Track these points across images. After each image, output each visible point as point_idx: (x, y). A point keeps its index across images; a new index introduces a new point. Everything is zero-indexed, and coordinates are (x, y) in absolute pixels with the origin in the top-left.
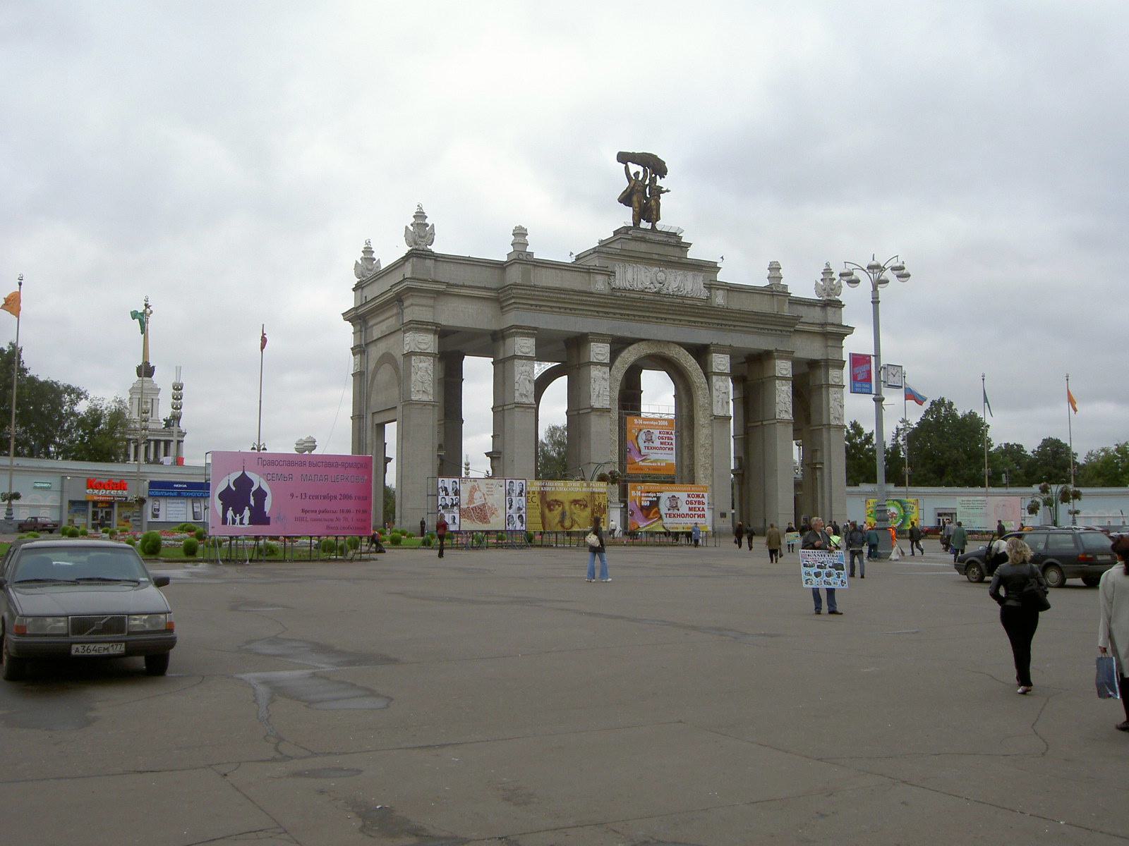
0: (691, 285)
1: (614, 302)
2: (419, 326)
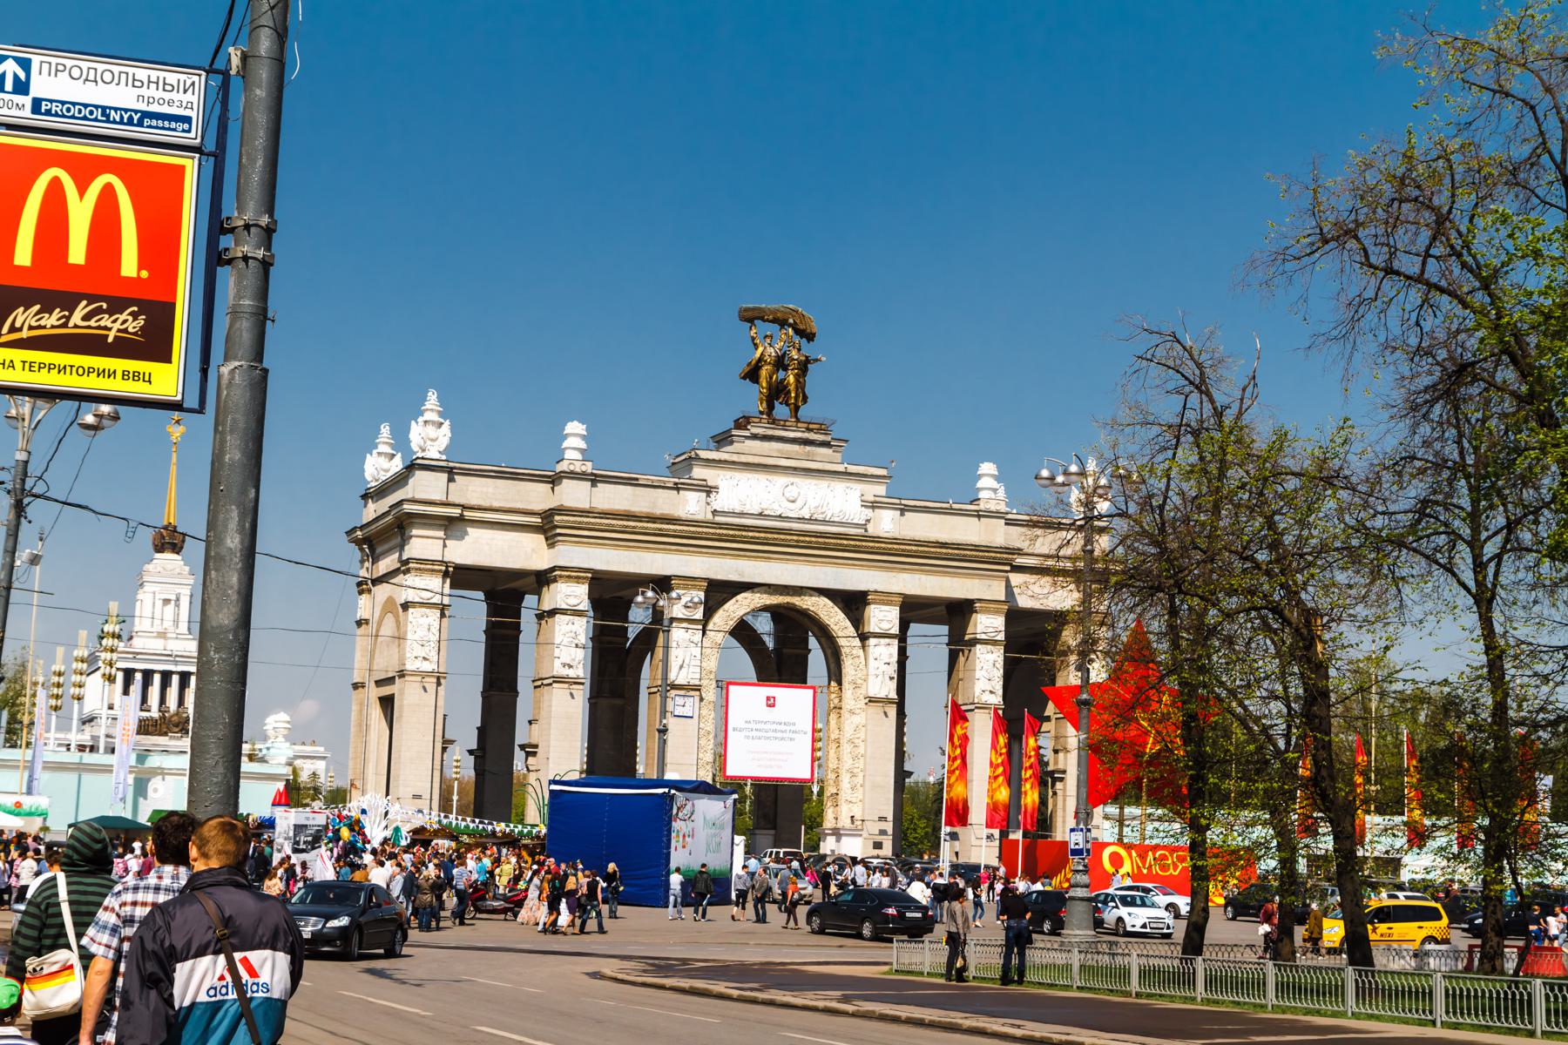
0: (839, 502)
2: (426, 566)
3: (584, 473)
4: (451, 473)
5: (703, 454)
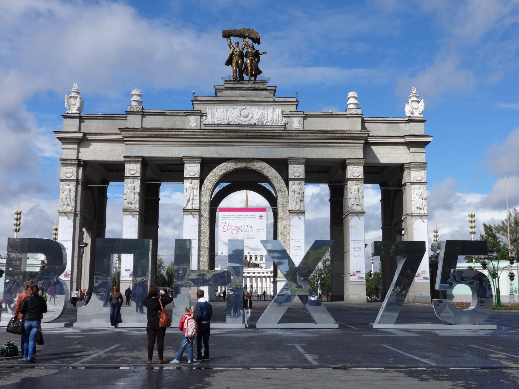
0: (271, 116)
1: (201, 133)
3: (138, 112)
4: (81, 119)
5: (199, 98)
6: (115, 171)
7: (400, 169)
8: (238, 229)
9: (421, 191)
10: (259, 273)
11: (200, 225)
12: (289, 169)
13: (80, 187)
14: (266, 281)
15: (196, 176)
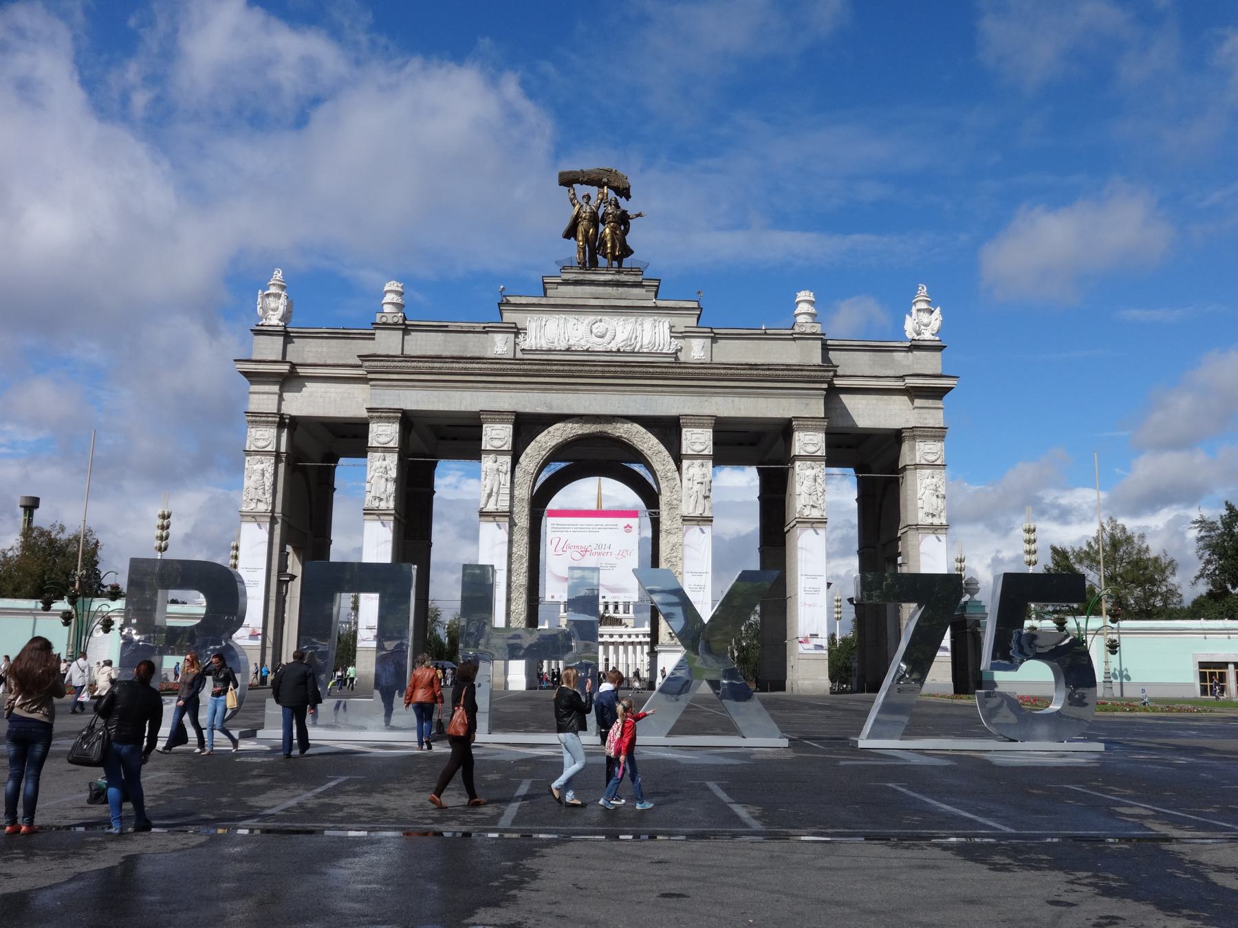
0: (650, 334)
3: (396, 324)
4: (287, 337)
5: (513, 300)
6: (349, 437)
7: (894, 438)
8: (584, 551)
9: (934, 480)
10: (621, 636)
11: (510, 542)
12: (683, 437)
13: (282, 466)
14: (635, 652)
15: (505, 448)
